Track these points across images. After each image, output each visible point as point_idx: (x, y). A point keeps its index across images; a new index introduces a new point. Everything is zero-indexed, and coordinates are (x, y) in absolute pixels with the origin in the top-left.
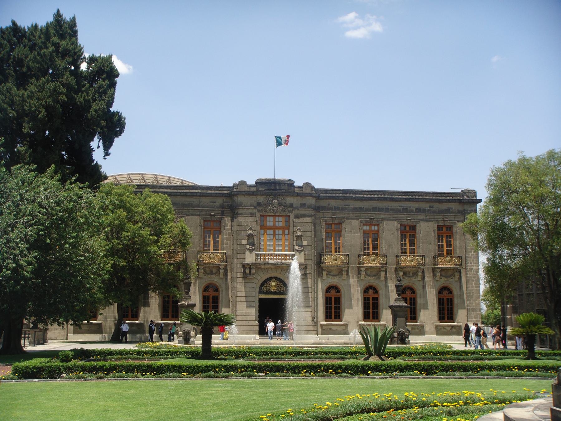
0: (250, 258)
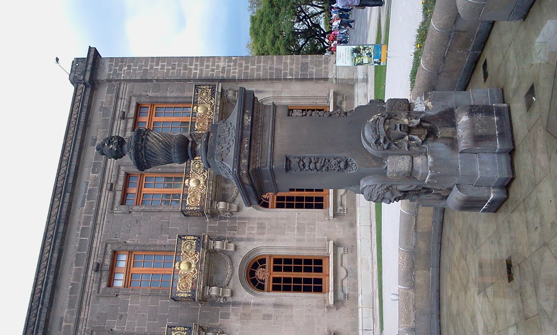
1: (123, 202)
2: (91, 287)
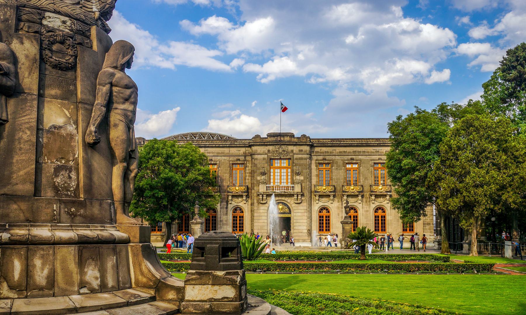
0: (262, 189)
1: (375, 163)
2: (346, 158)
